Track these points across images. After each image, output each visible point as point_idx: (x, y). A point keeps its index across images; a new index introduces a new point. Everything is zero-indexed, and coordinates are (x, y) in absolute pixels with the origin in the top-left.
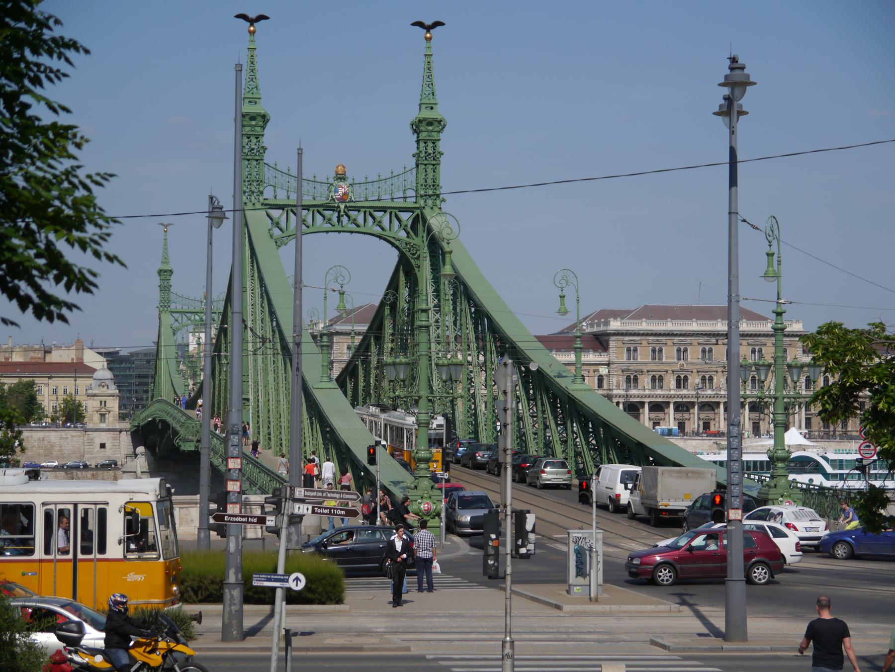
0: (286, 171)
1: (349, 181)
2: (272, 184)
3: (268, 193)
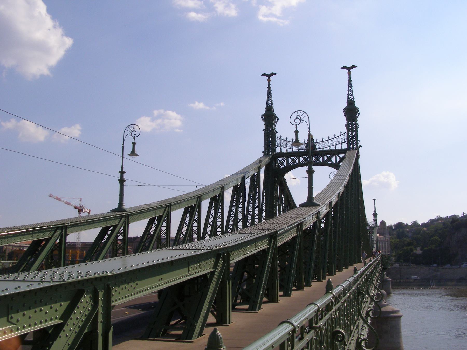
0: (286, 139)
1: (315, 141)
2: (279, 145)
3: (278, 150)
